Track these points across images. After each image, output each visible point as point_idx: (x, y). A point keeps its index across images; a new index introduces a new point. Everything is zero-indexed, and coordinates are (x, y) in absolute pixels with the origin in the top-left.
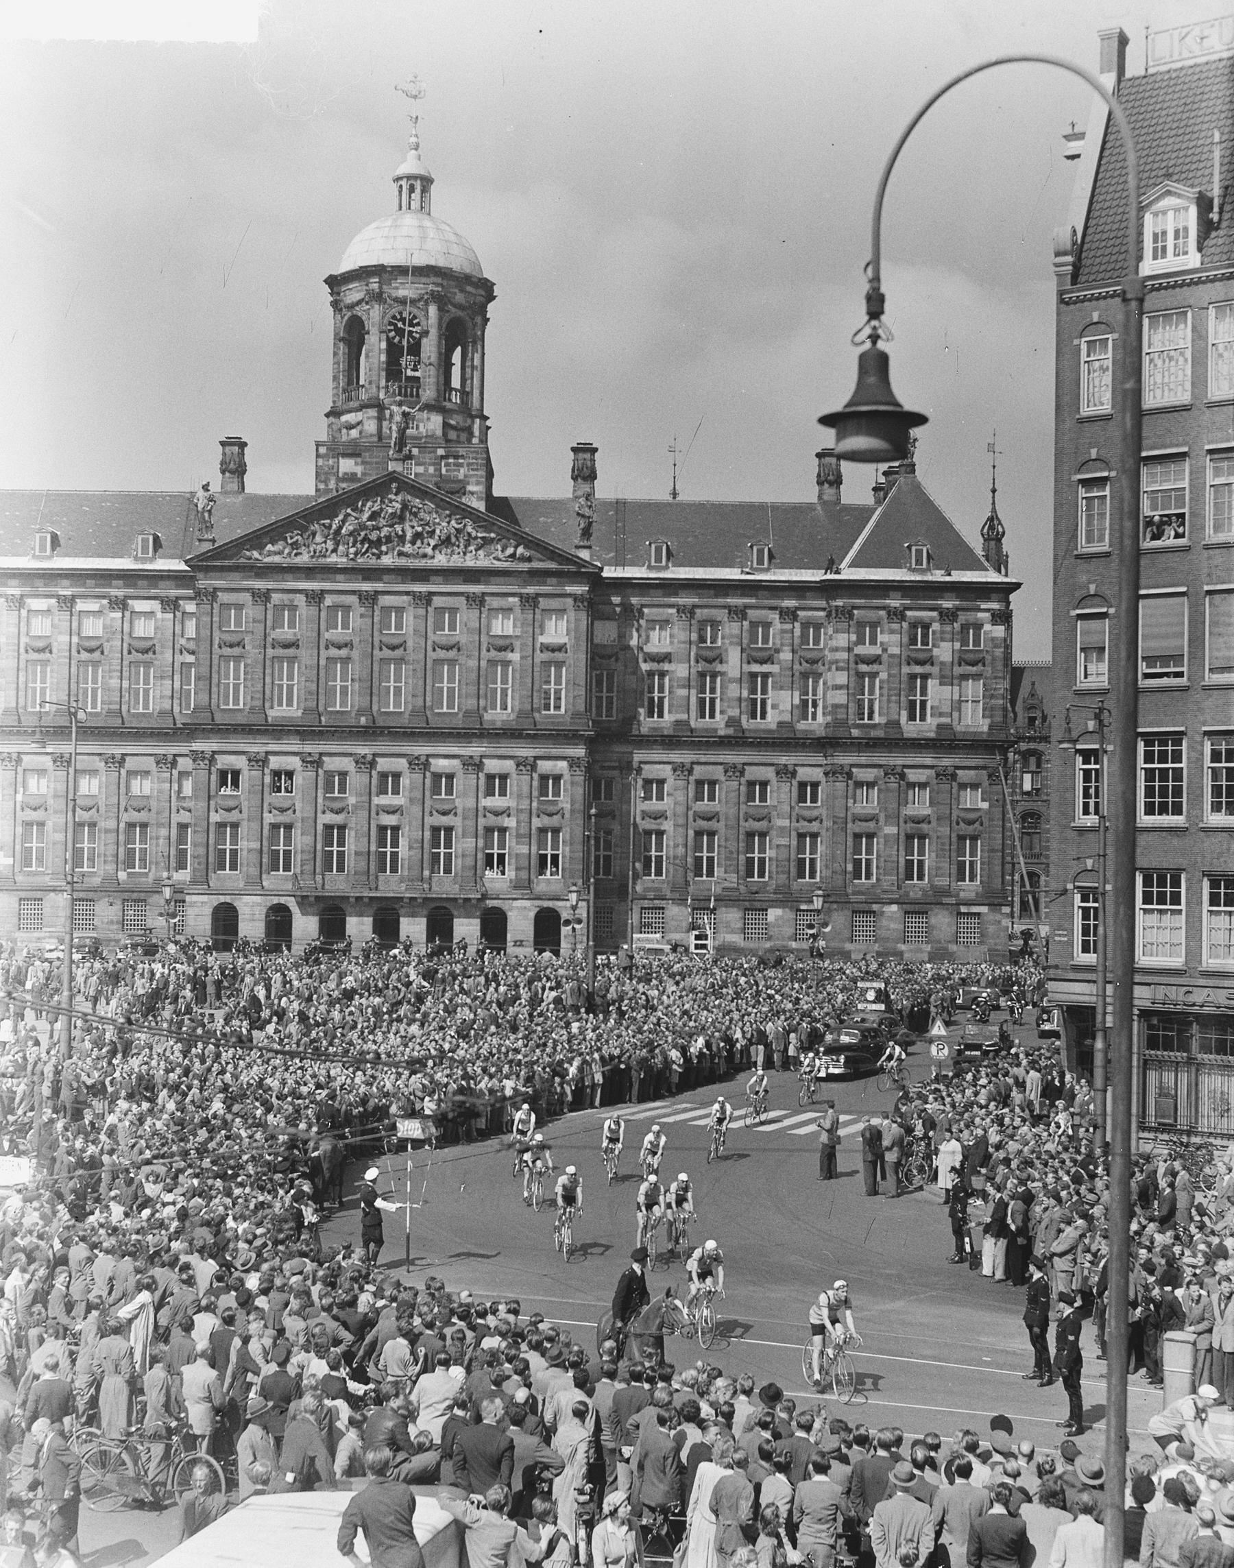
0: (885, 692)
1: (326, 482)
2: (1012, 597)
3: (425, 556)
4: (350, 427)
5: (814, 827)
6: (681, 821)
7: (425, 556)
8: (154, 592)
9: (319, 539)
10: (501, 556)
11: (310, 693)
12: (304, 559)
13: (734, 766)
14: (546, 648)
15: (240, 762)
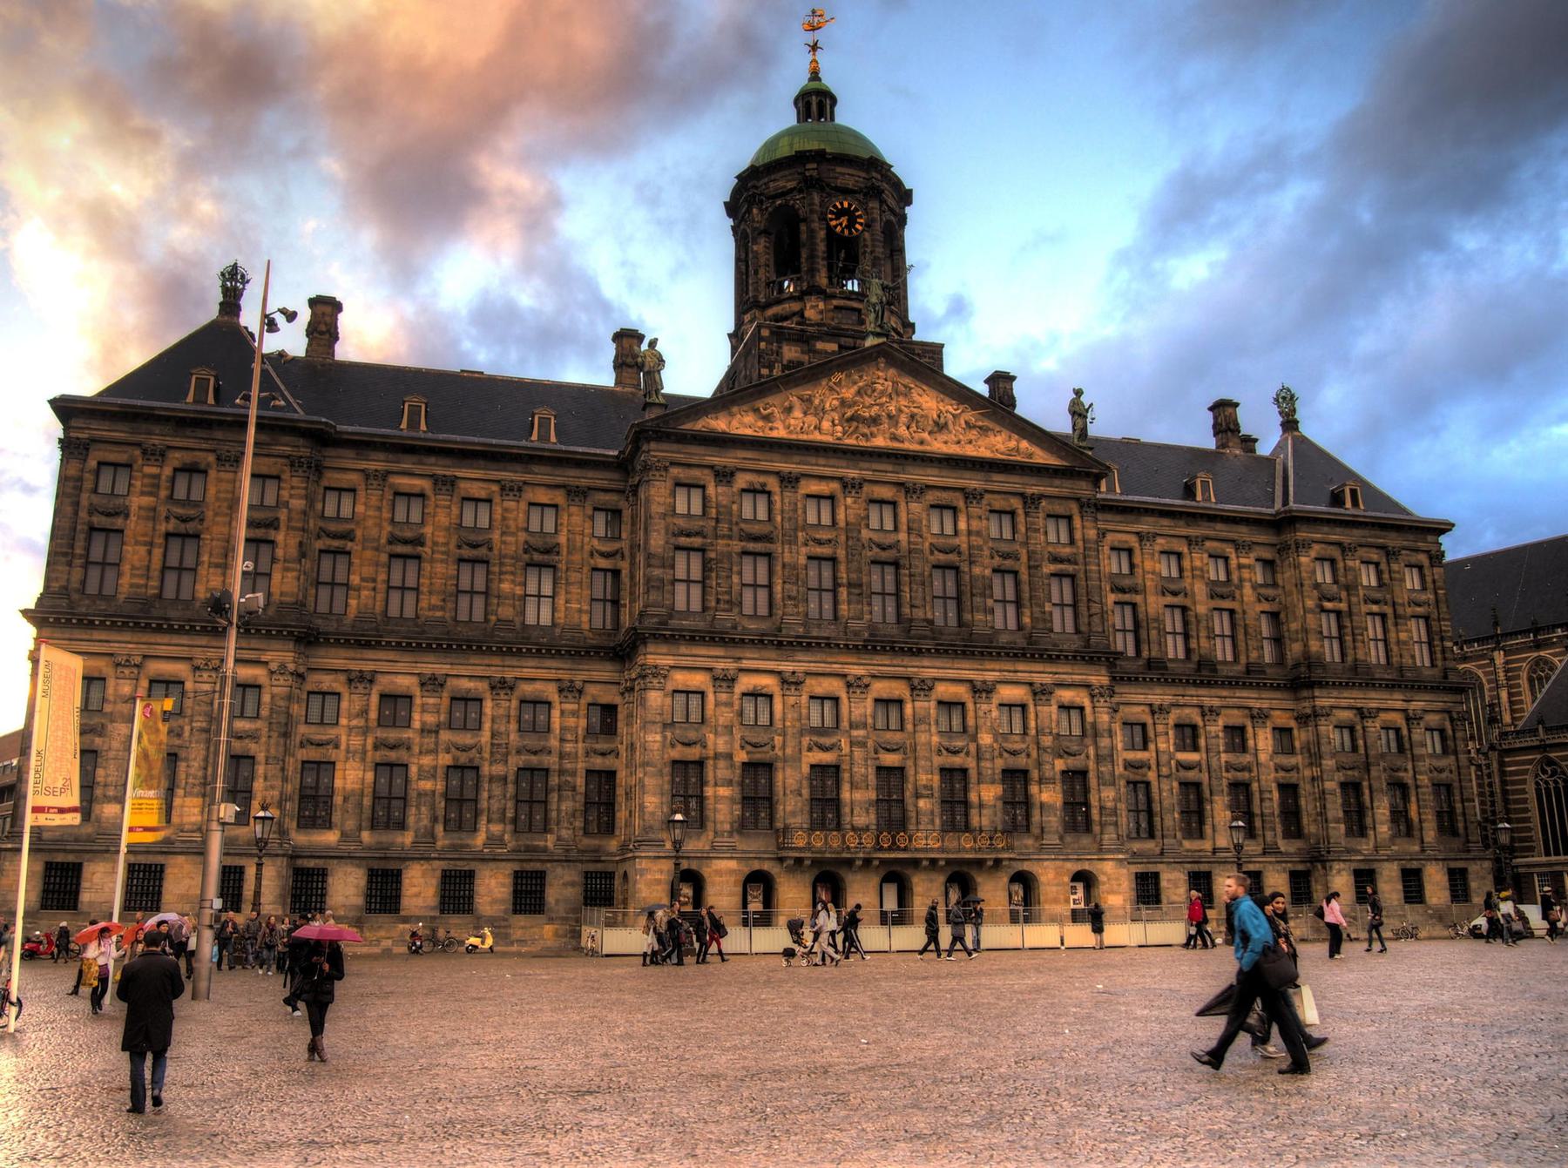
0: (1349, 630)
1: (771, 367)
2: (1442, 539)
3: (922, 443)
4: (785, 318)
5: (1292, 777)
6: (1164, 771)
7: (922, 443)
8: (559, 480)
9: (797, 413)
10: (1001, 447)
11: (790, 598)
12: (780, 433)
13: (1211, 710)
14: (1056, 559)
15: (698, 680)
